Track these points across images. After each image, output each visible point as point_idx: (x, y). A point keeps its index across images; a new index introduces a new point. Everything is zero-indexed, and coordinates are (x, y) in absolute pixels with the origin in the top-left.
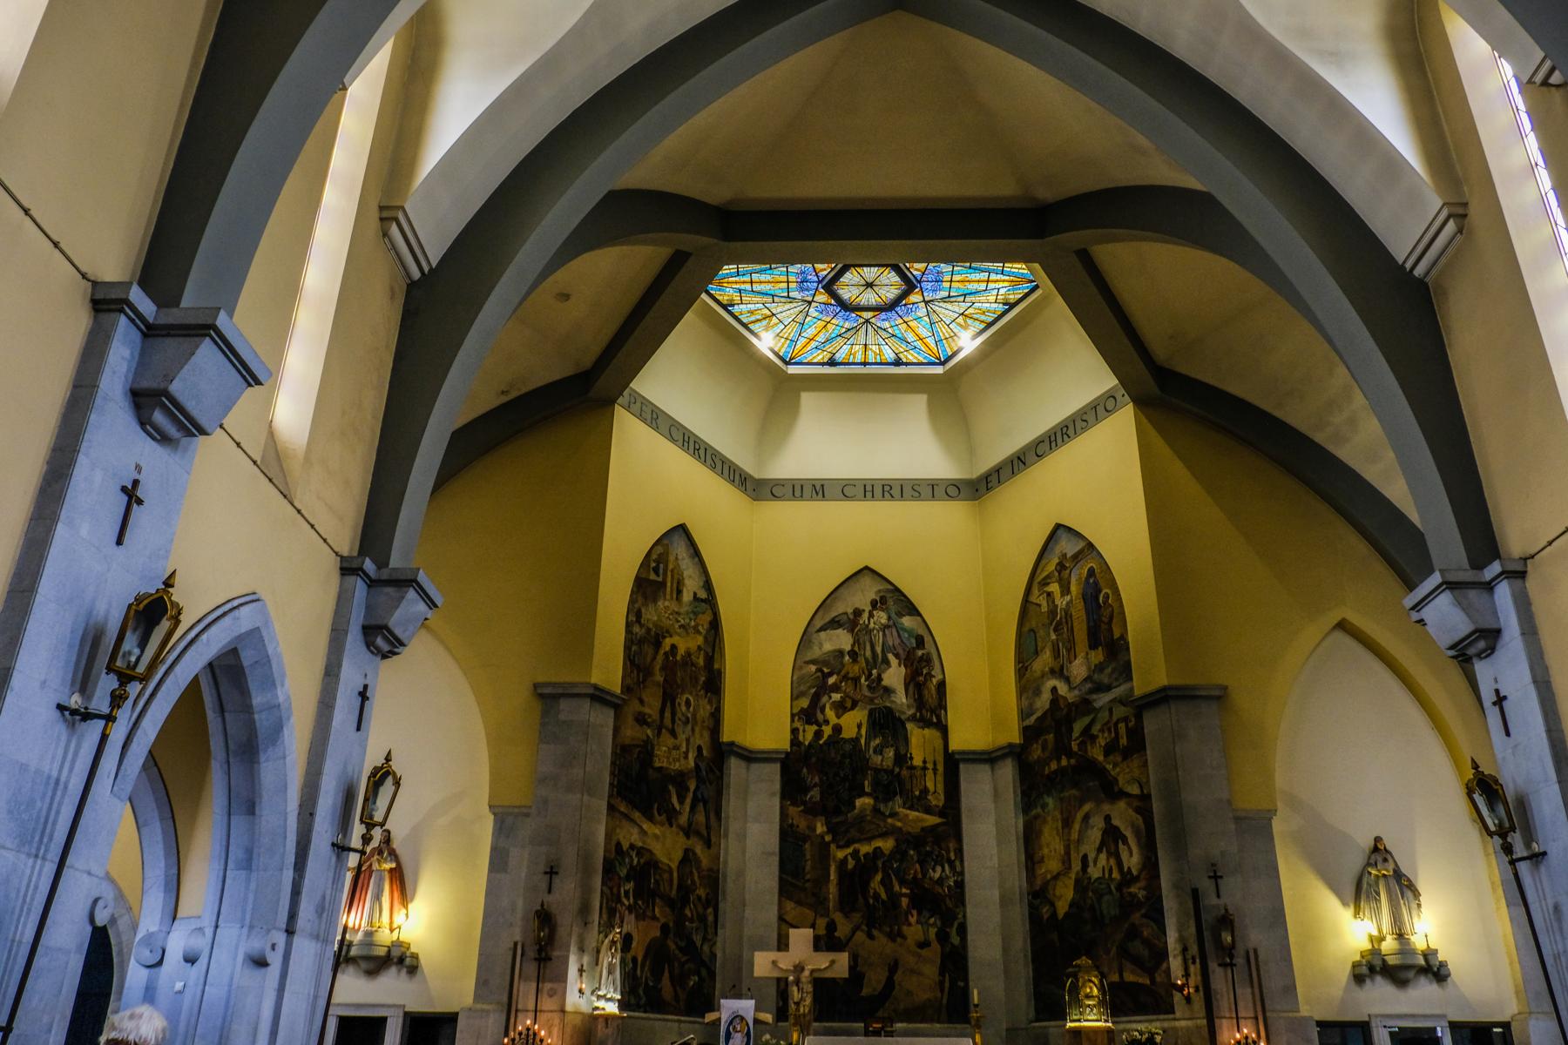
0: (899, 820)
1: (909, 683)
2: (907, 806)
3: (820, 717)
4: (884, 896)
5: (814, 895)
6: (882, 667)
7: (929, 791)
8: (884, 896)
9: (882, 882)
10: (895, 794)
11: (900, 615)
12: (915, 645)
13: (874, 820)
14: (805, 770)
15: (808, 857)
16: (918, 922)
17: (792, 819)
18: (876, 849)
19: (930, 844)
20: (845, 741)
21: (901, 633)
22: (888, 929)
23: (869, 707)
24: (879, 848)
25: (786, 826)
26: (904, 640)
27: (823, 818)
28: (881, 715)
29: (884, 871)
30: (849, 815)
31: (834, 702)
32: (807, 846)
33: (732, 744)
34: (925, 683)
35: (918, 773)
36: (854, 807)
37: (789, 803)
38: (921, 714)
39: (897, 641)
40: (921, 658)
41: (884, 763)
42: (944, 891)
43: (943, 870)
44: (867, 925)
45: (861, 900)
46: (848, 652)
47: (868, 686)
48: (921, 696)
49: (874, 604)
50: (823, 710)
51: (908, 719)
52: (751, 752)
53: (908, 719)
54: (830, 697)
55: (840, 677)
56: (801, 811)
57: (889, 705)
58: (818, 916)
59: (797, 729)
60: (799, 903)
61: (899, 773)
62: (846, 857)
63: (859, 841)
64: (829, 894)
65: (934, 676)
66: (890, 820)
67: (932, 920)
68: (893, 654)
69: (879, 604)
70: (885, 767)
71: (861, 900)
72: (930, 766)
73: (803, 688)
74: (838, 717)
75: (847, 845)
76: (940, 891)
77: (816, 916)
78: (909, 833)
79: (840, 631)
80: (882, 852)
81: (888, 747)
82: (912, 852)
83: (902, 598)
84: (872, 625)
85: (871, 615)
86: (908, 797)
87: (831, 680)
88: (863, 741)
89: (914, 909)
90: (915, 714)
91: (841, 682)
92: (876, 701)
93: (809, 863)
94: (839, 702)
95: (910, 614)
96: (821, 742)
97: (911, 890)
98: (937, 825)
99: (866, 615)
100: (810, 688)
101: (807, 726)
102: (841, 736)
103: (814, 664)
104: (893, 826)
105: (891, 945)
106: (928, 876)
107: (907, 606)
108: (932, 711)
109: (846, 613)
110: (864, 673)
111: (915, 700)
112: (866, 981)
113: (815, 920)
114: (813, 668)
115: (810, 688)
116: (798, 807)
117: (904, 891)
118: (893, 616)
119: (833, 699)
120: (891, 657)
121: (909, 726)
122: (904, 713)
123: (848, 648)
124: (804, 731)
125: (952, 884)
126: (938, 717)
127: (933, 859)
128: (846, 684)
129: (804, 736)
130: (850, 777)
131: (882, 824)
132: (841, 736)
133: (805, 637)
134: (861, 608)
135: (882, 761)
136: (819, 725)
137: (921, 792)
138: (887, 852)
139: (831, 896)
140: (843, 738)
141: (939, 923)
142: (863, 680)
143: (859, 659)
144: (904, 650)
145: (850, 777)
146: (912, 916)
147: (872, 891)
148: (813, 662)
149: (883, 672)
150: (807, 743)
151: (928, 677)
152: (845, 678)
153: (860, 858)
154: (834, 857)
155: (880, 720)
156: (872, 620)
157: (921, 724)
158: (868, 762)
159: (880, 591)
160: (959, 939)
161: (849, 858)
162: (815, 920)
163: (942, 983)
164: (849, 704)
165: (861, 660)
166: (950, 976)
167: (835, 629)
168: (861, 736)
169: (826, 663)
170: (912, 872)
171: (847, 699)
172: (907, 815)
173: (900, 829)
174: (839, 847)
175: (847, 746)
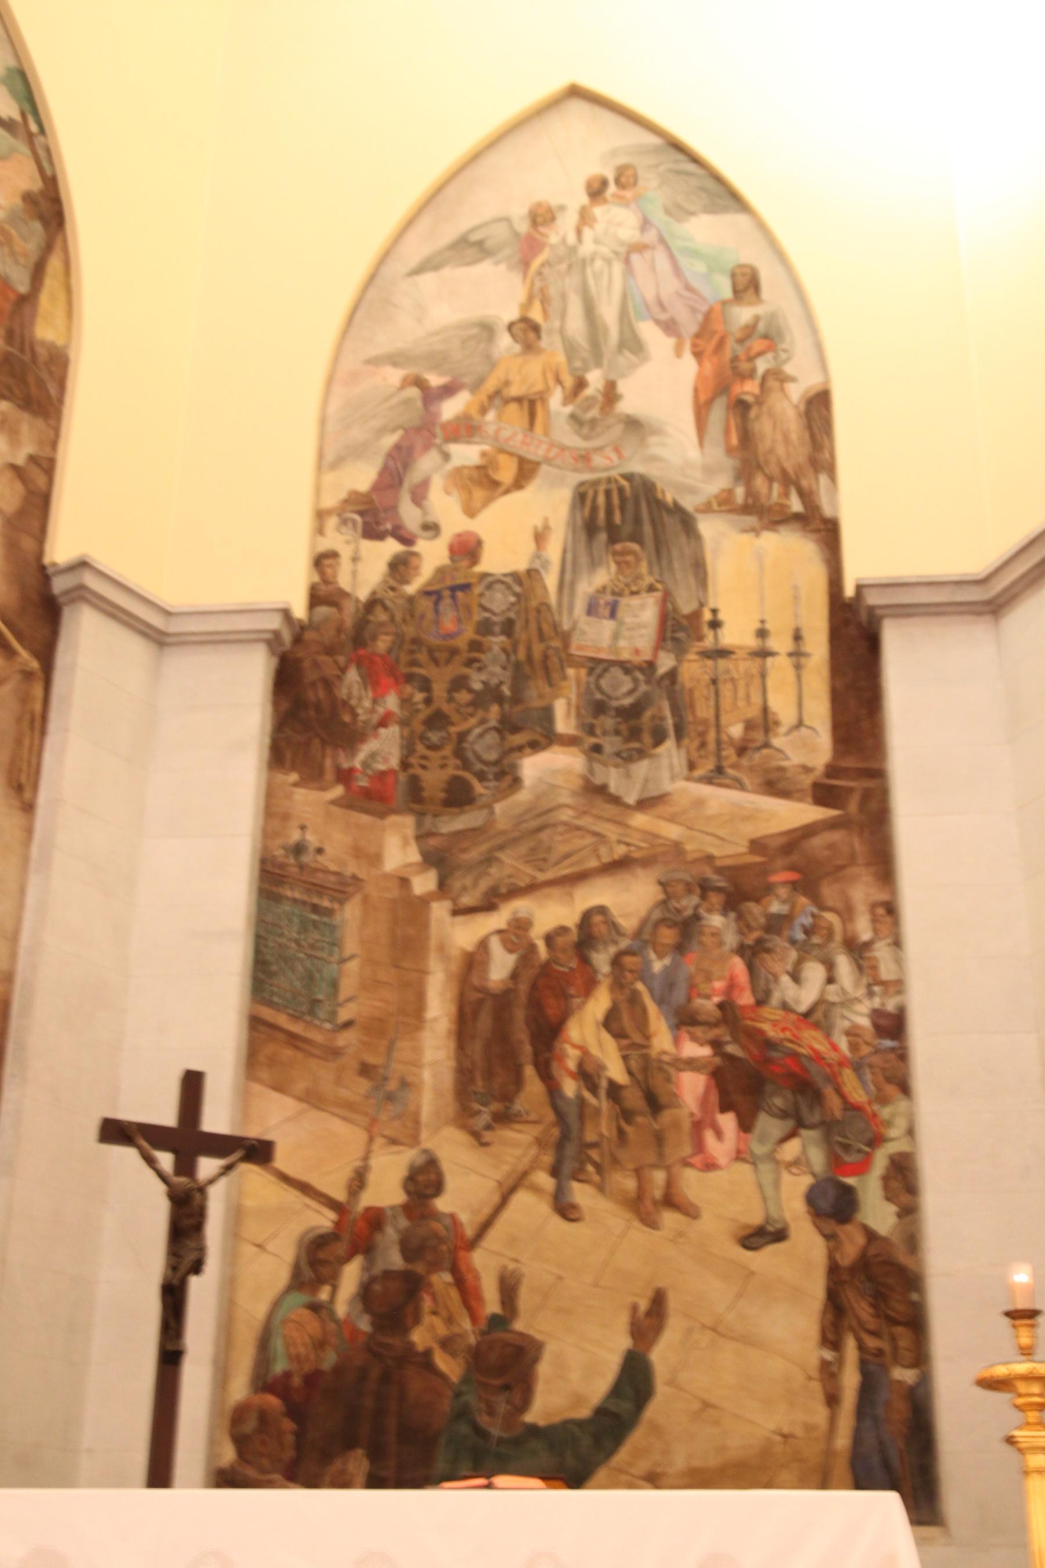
0: (672, 819)
1: (709, 402)
2: (698, 773)
3: (410, 515)
4: (616, 1071)
5: (365, 1070)
6: (621, 361)
7: (777, 723)
8: (616, 1071)
9: (610, 1022)
10: (659, 738)
11: (678, 212)
12: (727, 293)
13: (586, 822)
14: (353, 675)
15: (351, 945)
16: (739, 1156)
17: (303, 828)
18: (587, 916)
19: (783, 892)
20: (490, 581)
21: (684, 262)
22: (630, 1184)
23: (575, 478)
24: (602, 910)
25: (279, 853)
26: (695, 284)
27: (407, 823)
28: (616, 500)
29: (618, 984)
30: (498, 808)
31: (458, 471)
32: (350, 913)
33: (83, 564)
34: (760, 401)
35: (741, 667)
36: (516, 782)
37: (294, 777)
38: (750, 493)
39: (670, 286)
40: (750, 331)
41: (622, 643)
42: (835, 1048)
43: (830, 980)
44: (555, 1172)
45: (533, 1085)
46: (510, 327)
47: (573, 417)
48: (747, 438)
49: (597, 191)
50: (419, 496)
51: (707, 509)
52: (167, 613)
53: (707, 509)
54: (446, 457)
55: (482, 396)
56: (334, 802)
57: (637, 467)
58: (379, 1141)
59: (334, 555)
60: (313, 1099)
61: (672, 675)
62: (483, 944)
63: (531, 888)
64: (418, 1064)
65: (793, 379)
66: (640, 820)
67: (792, 1149)
68: (658, 322)
69: (612, 188)
70: (625, 656)
71: (533, 1085)
72: (780, 643)
73: (357, 434)
74: (471, 512)
75: (488, 906)
76: (822, 1047)
77: (371, 1140)
78: (709, 859)
79: (485, 268)
80: (614, 926)
81: (633, 593)
82: (716, 920)
83: (691, 167)
84: (587, 247)
85: (585, 218)
86: (703, 745)
87: (451, 409)
88: (551, 580)
89: (724, 1108)
90: (730, 492)
91: (484, 411)
92: (598, 460)
93: (353, 966)
94: (478, 468)
95: (712, 209)
96: (411, 589)
97: (716, 1045)
98: (808, 831)
99: (567, 223)
100: (381, 431)
101: (368, 546)
102: (479, 569)
103: (395, 365)
104: (653, 836)
105: (639, 1233)
106: (776, 998)
107: (703, 189)
108: (788, 481)
109: (507, 220)
110: (559, 381)
111: (729, 451)
112: (544, 1369)
113: (366, 1158)
114: (394, 376)
115: (381, 431)
116: (323, 789)
117: (695, 1050)
118: (658, 216)
119: (456, 461)
120: (649, 332)
121: (708, 527)
122: (693, 491)
123: (512, 313)
124: (355, 559)
125: (865, 1022)
126: (805, 496)
127: (793, 942)
128: (499, 417)
129: (354, 573)
130: (506, 690)
131: (611, 831)
132: (479, 569)
133: (371, 294)
134: (554, 201)
135: (616, 636)
136: (407, 540)
137: (749, 726)
138: (628, 924)
139: (427, 1075)
140: (485, 575)
141: (817, 1158)
142: (556, 400)
143: (544, 342)
144: (693, 310)
145: (506, 690)
146: (719, 1134)
147: (572, 1058)
148: (394, 359)
149: (623, 376)
150: (363, 594)
151: (772, 383)
152: (498, 397)
153: (532, 948)
154: (441, 948)
155: (609, 512)
156: (587, 233)
157: (751, 520)
158: (566, 645)
159: (614, 153)
160: (892, 1209)
161: (495, 944)
162: (366, 1158)
163: (829, 1373)
164: (506, 473)
165: (551, 343)
166: (861, 1347)
167: (469, 264)
168: (546, 564)
169: (437, 360)
170: (719, 985)
171: (502, 458)
172: (699, 803)
173: (677, 848)
174: (456, 912)
175: (498, 596)
